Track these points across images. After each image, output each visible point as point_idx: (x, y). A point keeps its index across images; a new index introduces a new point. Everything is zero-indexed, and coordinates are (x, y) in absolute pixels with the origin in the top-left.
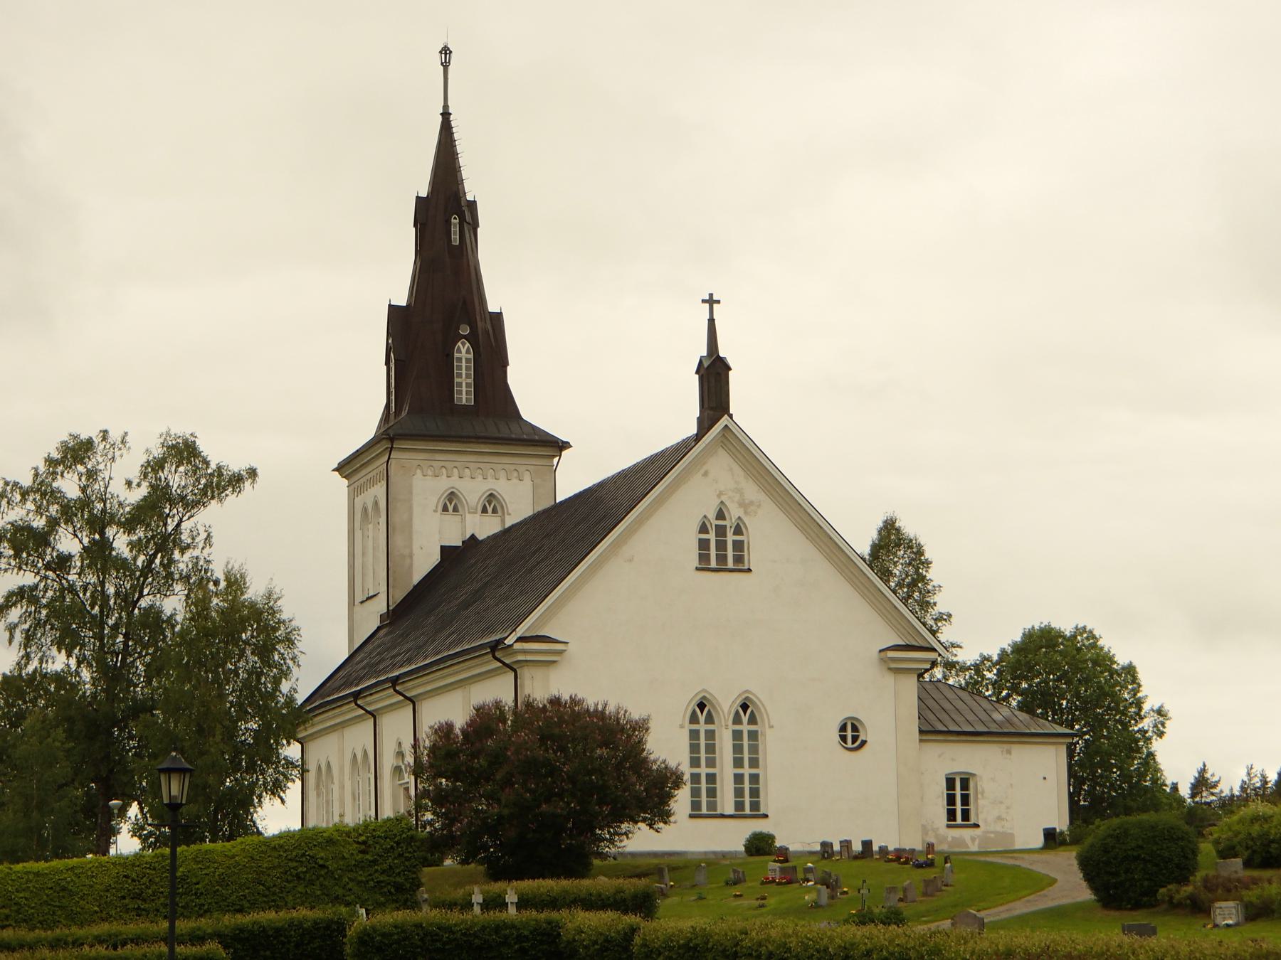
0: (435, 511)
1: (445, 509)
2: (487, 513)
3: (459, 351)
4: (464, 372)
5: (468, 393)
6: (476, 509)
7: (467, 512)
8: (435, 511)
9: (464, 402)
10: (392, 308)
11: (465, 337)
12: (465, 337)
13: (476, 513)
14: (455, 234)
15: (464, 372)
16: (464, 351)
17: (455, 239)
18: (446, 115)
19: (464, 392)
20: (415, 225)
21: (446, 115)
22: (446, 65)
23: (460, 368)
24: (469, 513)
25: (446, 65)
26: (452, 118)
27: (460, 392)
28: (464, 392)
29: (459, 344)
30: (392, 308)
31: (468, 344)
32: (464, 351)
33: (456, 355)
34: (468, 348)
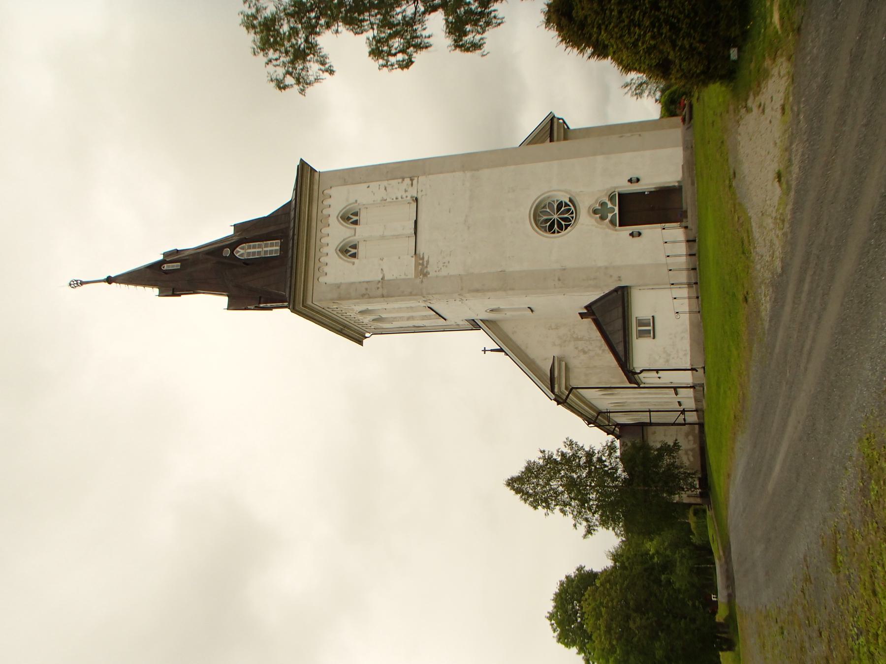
0: (354, 264)
1: (354, 256)
2: (357, 220)
3: (242, 255)
4: (257, 250)
5: (272, 245)
6: (353, 228)
7: (354, 238)
8: (354, 264)
9: (278, 248)
10: (232, 306)
11: (232, 252)
12: (232, 252)
13: (355, 229)
14: (174, 266)
15: (257, 250)
16: (242, 251)
17: (177, 266)
18: (109, 280)
19: (272, 248)
20: (179, 295)
21: (109, 280)
22: (82, 283)
23: (254, 253)
24: (355, 235)
25: (82, 283)
26: (113, 276)
27: (271, 251)
28: (272, 248)
29: (237, 255)
30: (232, 306)
31: (238, 249)
32: (242, 251)
33: (245, 257)
34: (240, 248)
